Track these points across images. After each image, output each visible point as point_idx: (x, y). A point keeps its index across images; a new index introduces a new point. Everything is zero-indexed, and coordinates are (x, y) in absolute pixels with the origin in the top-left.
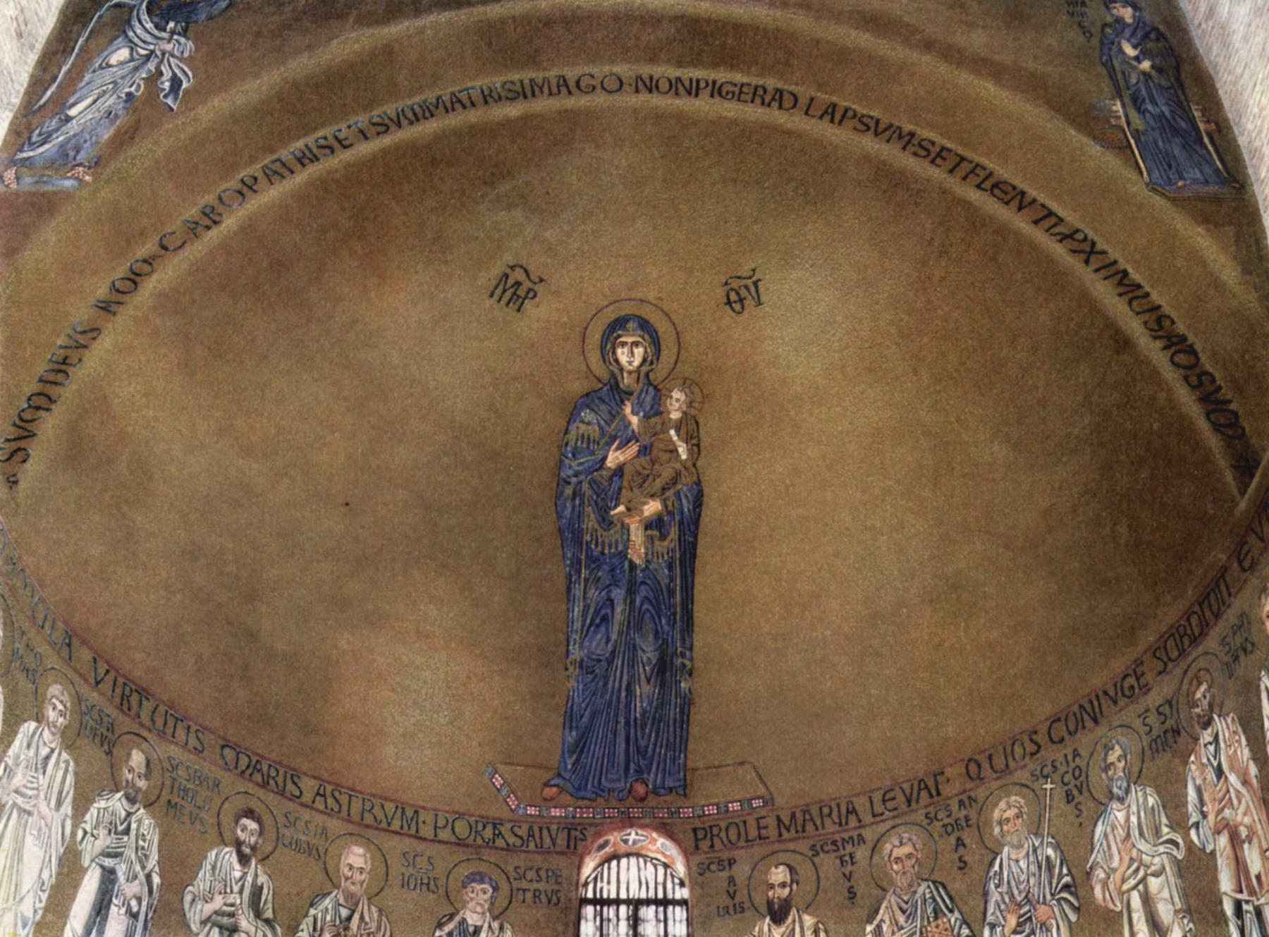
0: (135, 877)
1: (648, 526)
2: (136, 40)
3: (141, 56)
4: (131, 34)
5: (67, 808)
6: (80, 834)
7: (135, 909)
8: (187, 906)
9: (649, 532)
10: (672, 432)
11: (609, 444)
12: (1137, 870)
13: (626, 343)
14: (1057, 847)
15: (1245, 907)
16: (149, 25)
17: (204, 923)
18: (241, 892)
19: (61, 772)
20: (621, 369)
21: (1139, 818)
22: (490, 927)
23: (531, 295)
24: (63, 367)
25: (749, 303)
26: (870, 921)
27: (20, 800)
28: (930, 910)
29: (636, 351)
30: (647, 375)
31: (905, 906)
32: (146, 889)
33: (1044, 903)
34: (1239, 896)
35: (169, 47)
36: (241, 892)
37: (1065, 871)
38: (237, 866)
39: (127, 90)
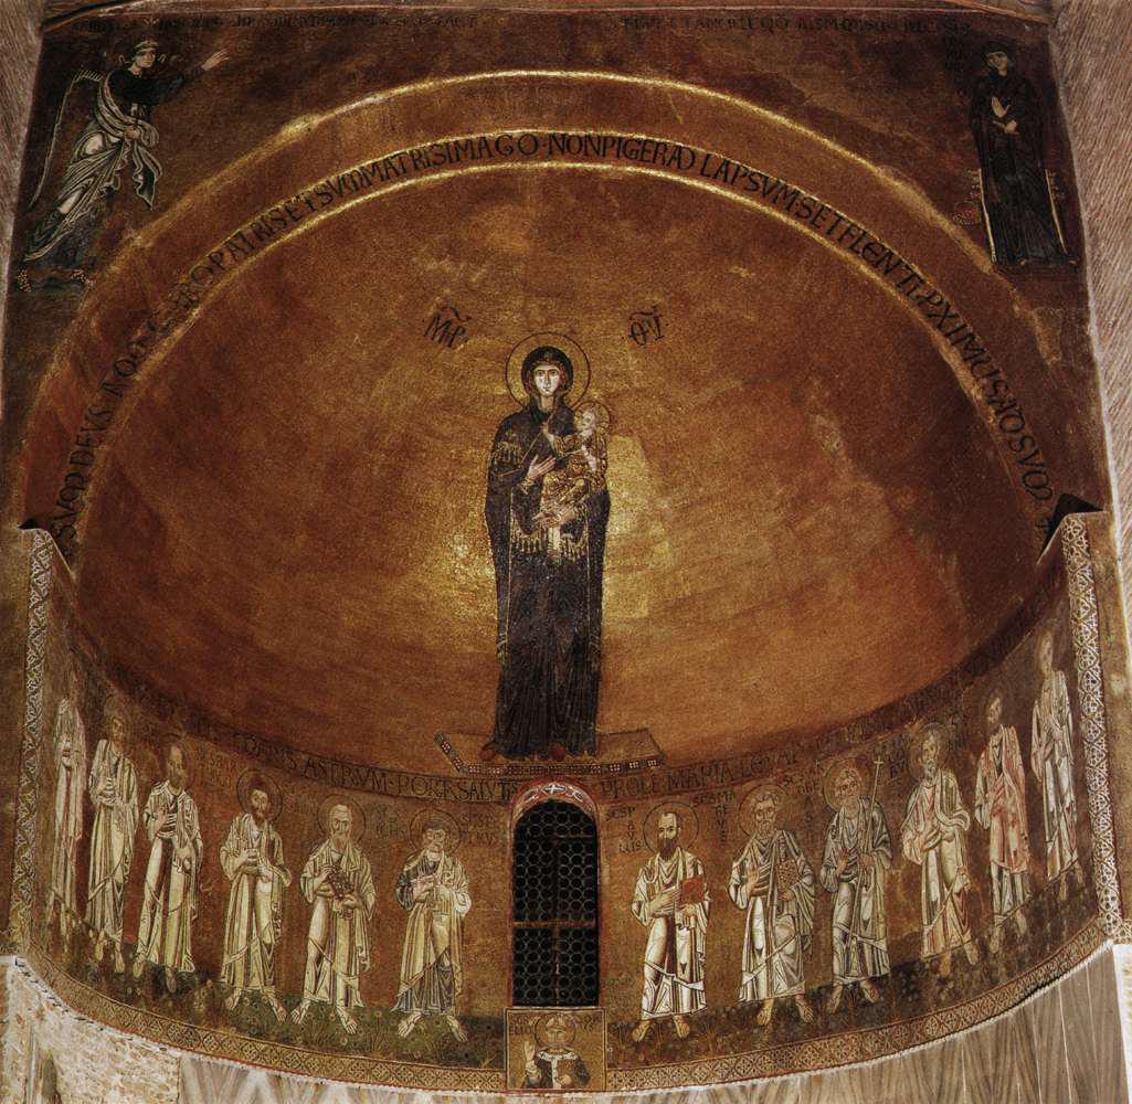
0: (185, 844)
1: (564, 529)
2: (105, 125)
3: (113, 144)
4: (100, 118)
5: (135, 800)
6: (145, 816)
7: (188, 868)
8: (223, 862)
9: (564, 535)
10: (584, 448)
11: (529, 459)
12: (937, 834)
13: (544, 371)
14: (881, 811)
15: (1005, 873)
16: (115, 108)
17: (236, 872)
18: (259, 846)
19: (128, 778)
20: (539, 395)
21: (941, 795)
22: (445, 862)
23: (460, 330)
24: (87, 449)
25: (652, 336)
26: (736, 859)
27: (104, 800)
28: (782, 852)
29: (552, 378)
30: (562, 398)
31: (764, 848)
32: (193, 851)
33: (867, 853)
34: (1002, 864)
35: (136, 133)
36: (259, 846)
37: (884, 830)
38: (255, 828)
39: (106, 184)
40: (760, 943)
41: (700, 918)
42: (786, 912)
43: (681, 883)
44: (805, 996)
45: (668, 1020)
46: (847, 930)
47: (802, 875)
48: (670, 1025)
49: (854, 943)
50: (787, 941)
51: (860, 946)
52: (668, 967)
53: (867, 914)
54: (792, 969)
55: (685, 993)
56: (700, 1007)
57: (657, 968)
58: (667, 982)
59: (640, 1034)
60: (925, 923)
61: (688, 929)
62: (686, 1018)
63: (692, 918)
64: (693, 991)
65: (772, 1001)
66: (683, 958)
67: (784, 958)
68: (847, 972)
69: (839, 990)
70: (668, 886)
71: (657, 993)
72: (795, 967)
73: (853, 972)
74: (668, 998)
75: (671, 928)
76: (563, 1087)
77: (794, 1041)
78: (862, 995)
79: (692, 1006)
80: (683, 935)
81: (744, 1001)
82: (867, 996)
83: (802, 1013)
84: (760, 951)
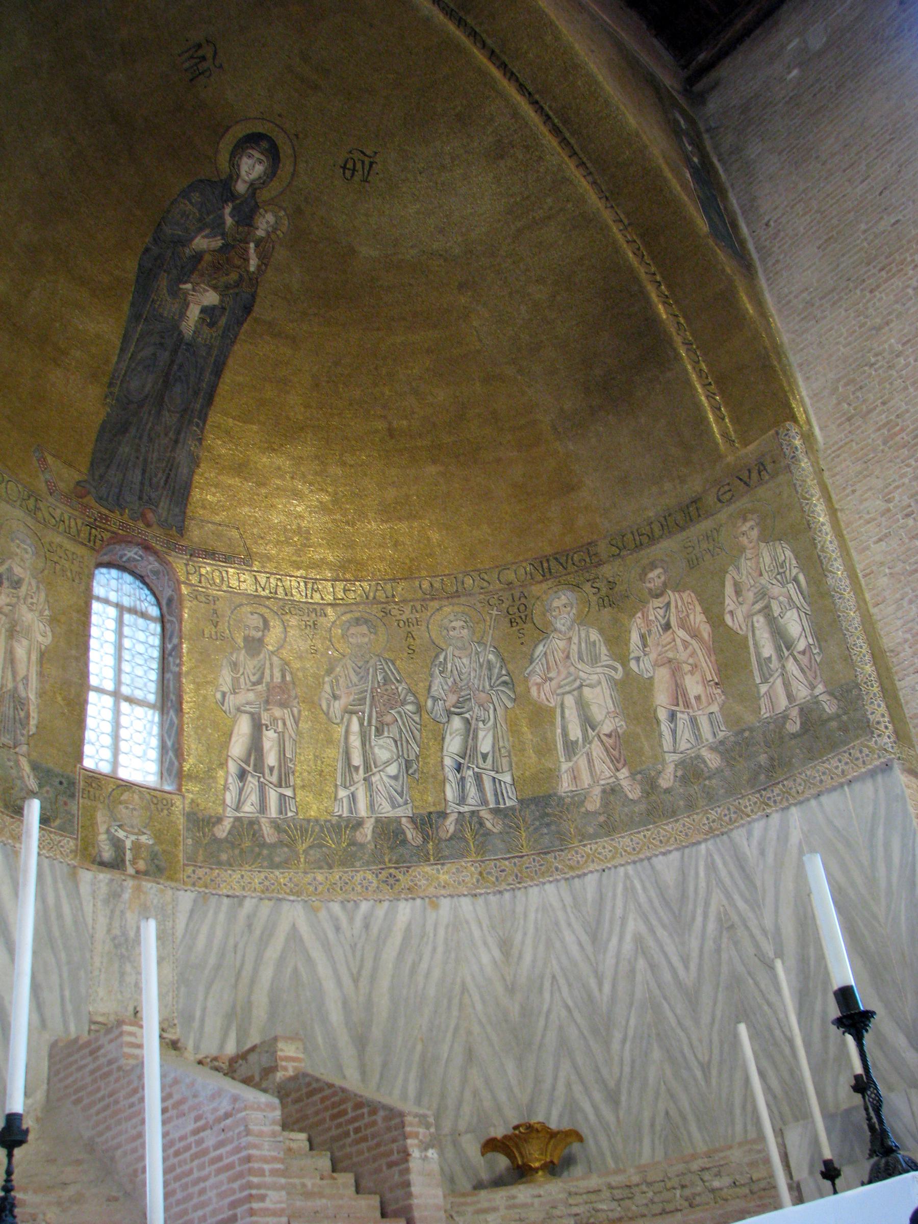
40: (357, 760)
41: (288, 723)
42: (386, 734)
43: (268, 684)
44: (412, 819)
45: (252, 823)
46: (462, 761)
47: (404, 703)
48: (256, 827)
49: (470, 773)
50: (388, 763)
51: (478, 778)
52: (255, 765)
53: (485, 746)
54: (396, 791)
55: (273, 797)
56: (290, 814)
57: (244, 765)
58: (252, 782)
59: (222, 831)
60: (563, 760)
61: (275, 732)
62: (276, 825)
63: (280, 723)
64: (282, 797)
65: (373, 820)
66: (271, 759)
67: (385, 778)
68: (462, 800)
69: (452, 818)
70: (254, 684)
71: (241, 790)
72: (399, 789)
73: (470, 801)
74: (254, 798)
75: (258, 728)
76: (138, 872)
77: (404, 864)
78: (481, 824)
79: (281, 813)
80: (269, 739)
81: (340, 816)
82: (489, 825)
83: (409, 836)
84: (357, 768)
